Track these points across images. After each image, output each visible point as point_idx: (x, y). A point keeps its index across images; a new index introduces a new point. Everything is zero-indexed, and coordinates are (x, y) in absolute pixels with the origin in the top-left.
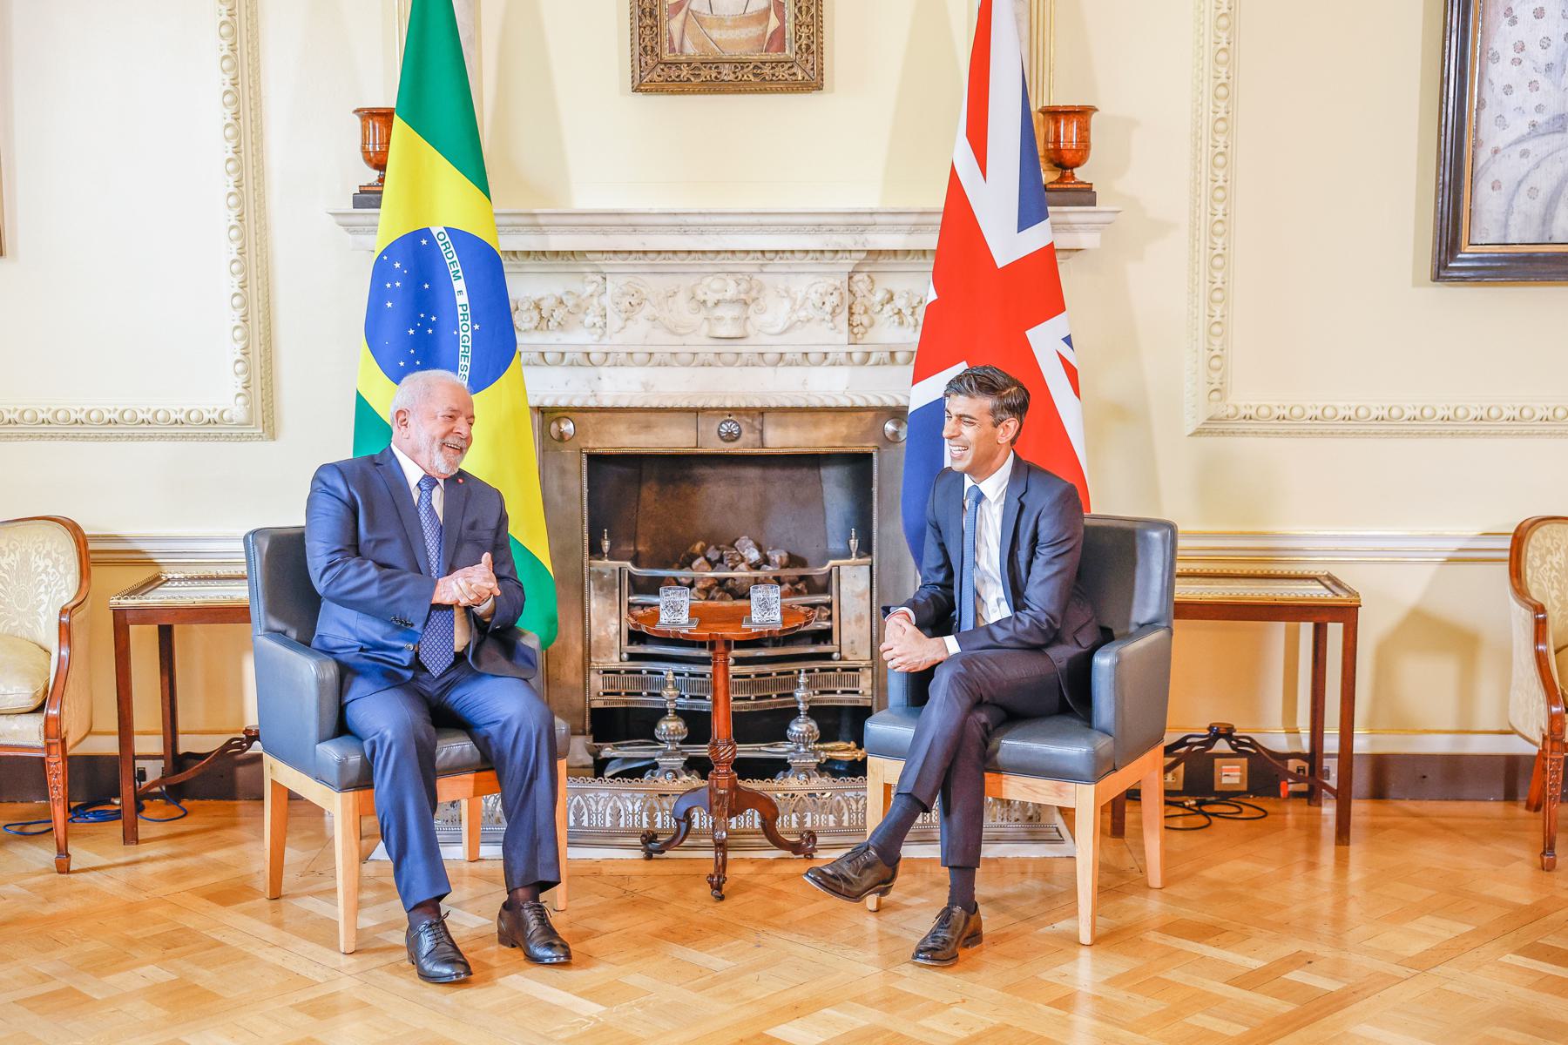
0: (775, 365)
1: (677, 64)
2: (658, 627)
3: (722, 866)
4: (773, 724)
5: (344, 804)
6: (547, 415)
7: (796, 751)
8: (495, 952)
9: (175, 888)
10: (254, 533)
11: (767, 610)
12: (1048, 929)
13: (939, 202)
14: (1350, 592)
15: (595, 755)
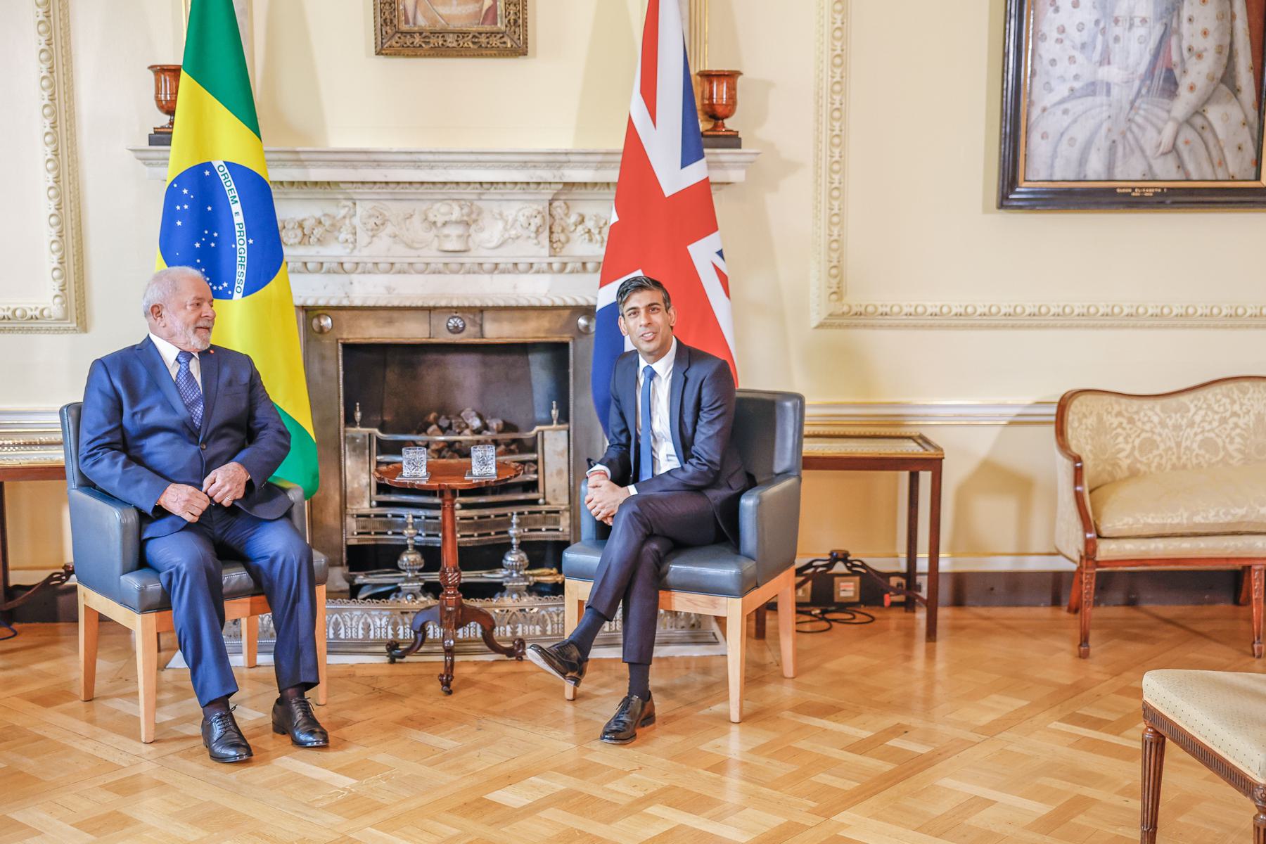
0: (491, 272)
1: (411, 34)
2: (398, 479)
3: (450, 667)
4: (492, 555)
5: (144, 623)
6: (309, 313)
7: (510, 576)
8: (270, 741)
9: (6, 694)
10: (68, 406)
11: (484, 465)
12: (706, 711)
13: (620, 146)
14: (937, 448)
15: (350, 580)
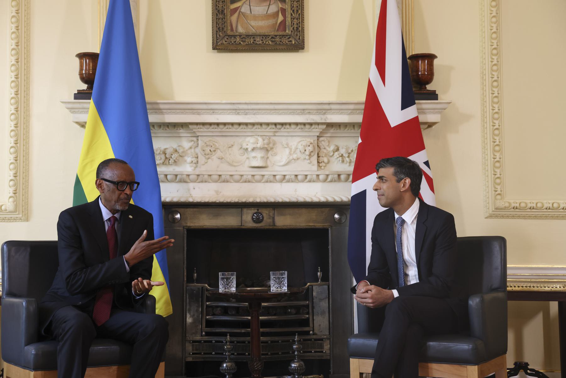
1: (235, 36)
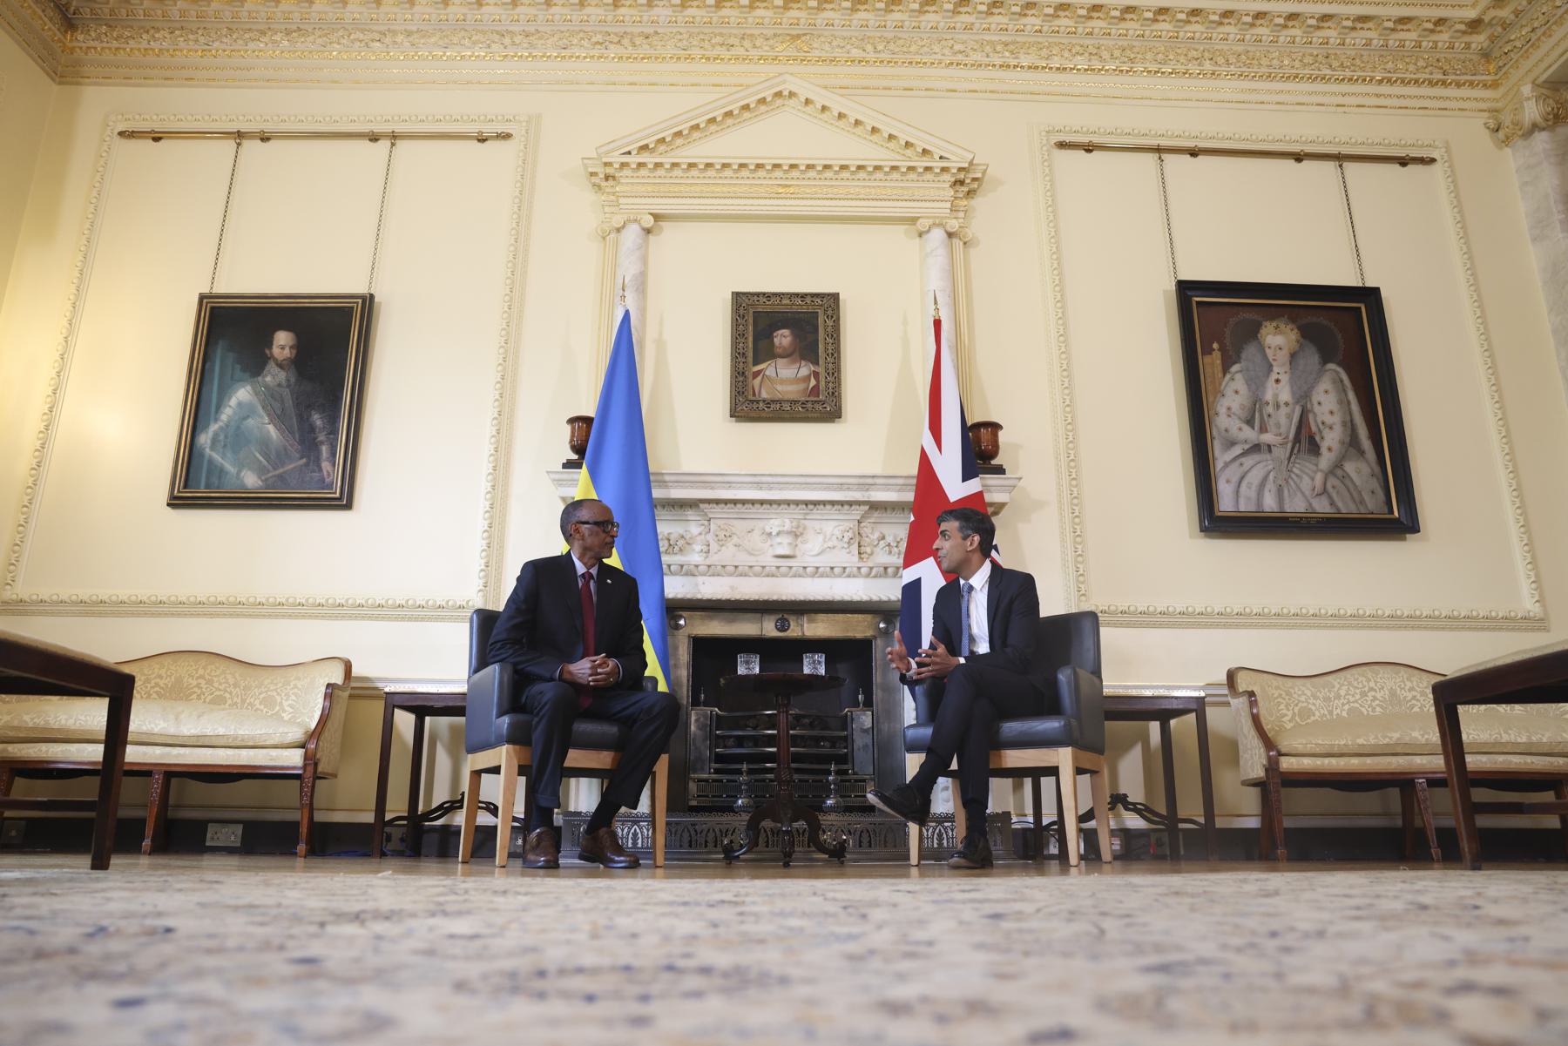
0: (813, 576)
